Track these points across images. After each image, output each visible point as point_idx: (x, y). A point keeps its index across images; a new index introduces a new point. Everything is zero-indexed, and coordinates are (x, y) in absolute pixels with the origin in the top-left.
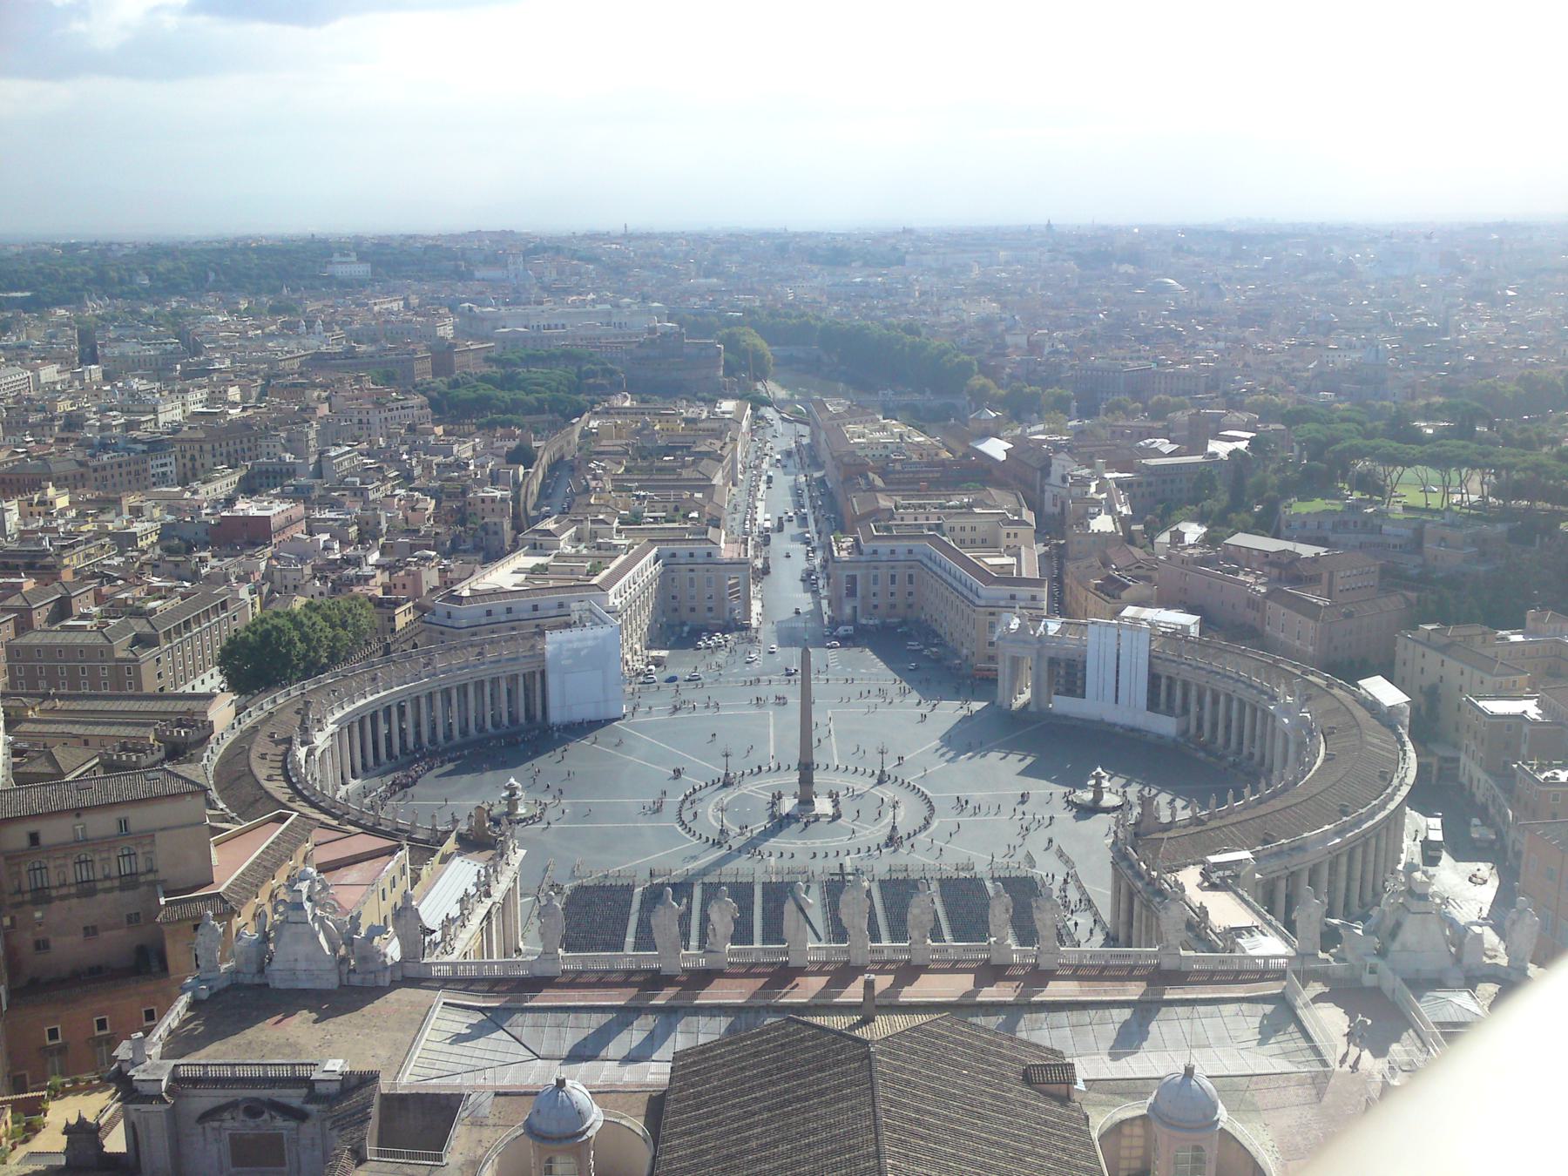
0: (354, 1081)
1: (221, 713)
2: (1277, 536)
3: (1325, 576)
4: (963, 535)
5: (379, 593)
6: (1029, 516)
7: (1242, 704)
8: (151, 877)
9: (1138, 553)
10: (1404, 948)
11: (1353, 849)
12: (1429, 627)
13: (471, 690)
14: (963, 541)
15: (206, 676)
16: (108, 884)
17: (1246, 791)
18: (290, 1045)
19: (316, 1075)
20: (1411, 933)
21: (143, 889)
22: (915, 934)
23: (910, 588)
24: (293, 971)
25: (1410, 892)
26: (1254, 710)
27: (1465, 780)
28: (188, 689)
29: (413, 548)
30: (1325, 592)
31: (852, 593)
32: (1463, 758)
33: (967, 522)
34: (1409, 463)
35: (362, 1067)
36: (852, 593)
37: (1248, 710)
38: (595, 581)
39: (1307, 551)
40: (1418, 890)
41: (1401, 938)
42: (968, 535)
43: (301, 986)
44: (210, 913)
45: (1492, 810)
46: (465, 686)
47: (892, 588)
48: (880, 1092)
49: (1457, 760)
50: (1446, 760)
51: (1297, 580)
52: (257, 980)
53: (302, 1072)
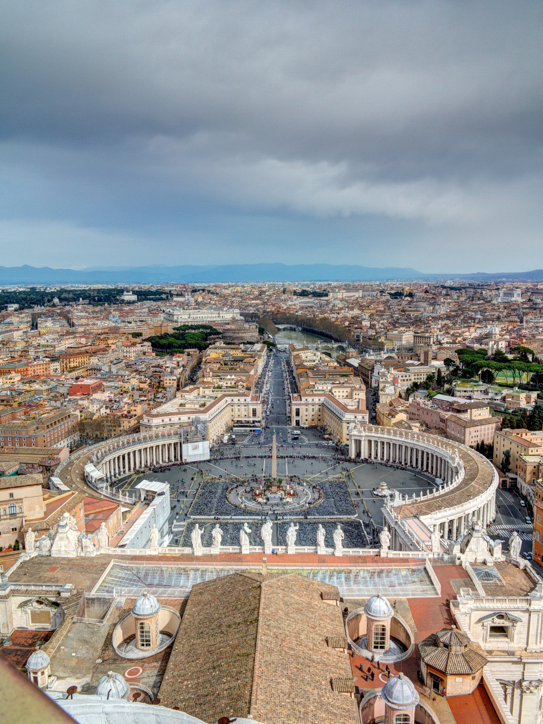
0: (75, 592)
1: (64, 455)
2: (453, 396)
3: (469, 411)
4: (339, 394)
5: (125, 413)
6: (364, 387)
7: (437, 457)
8: (21, 515)
9: (402, 401)
10: (471, 550)
11: (474, 512)
12: (506, 430)
13: (154, 448)
14: (339, 396)
15: (62, 442)
16: (5, 517)
17: (434, 490)
18: (54, 578)
19: (61, 590)
20: (472, 545)
21: (18, 519)
22: (289, 543)
23: (319, 413)
24: (60, 551)
25: (473, 529)
26: (441, 460)
27: (519, 486)
28: (55, 446)
29: (140, 396)
30: (469, 417)
31: (298, 414)
32: (519, 479)
33: (341, 390)
34: (499, 369)
35: (79, 587)
36: (298, 414)
37: (439, 459)
38: (202, 409)
39: (462, 401)
40: (476, 528)
41: (469, 546)
42: (341, 394)
43: (63, 556)
44: (30, 529)
45: (528, 497)
46: (152, 447)
47: (313, 413)
48: (262, 601)
49: (516, 479)
50: (512, 479)
51: (459, 411)
52: (48, 554)
53: (58, 589)
